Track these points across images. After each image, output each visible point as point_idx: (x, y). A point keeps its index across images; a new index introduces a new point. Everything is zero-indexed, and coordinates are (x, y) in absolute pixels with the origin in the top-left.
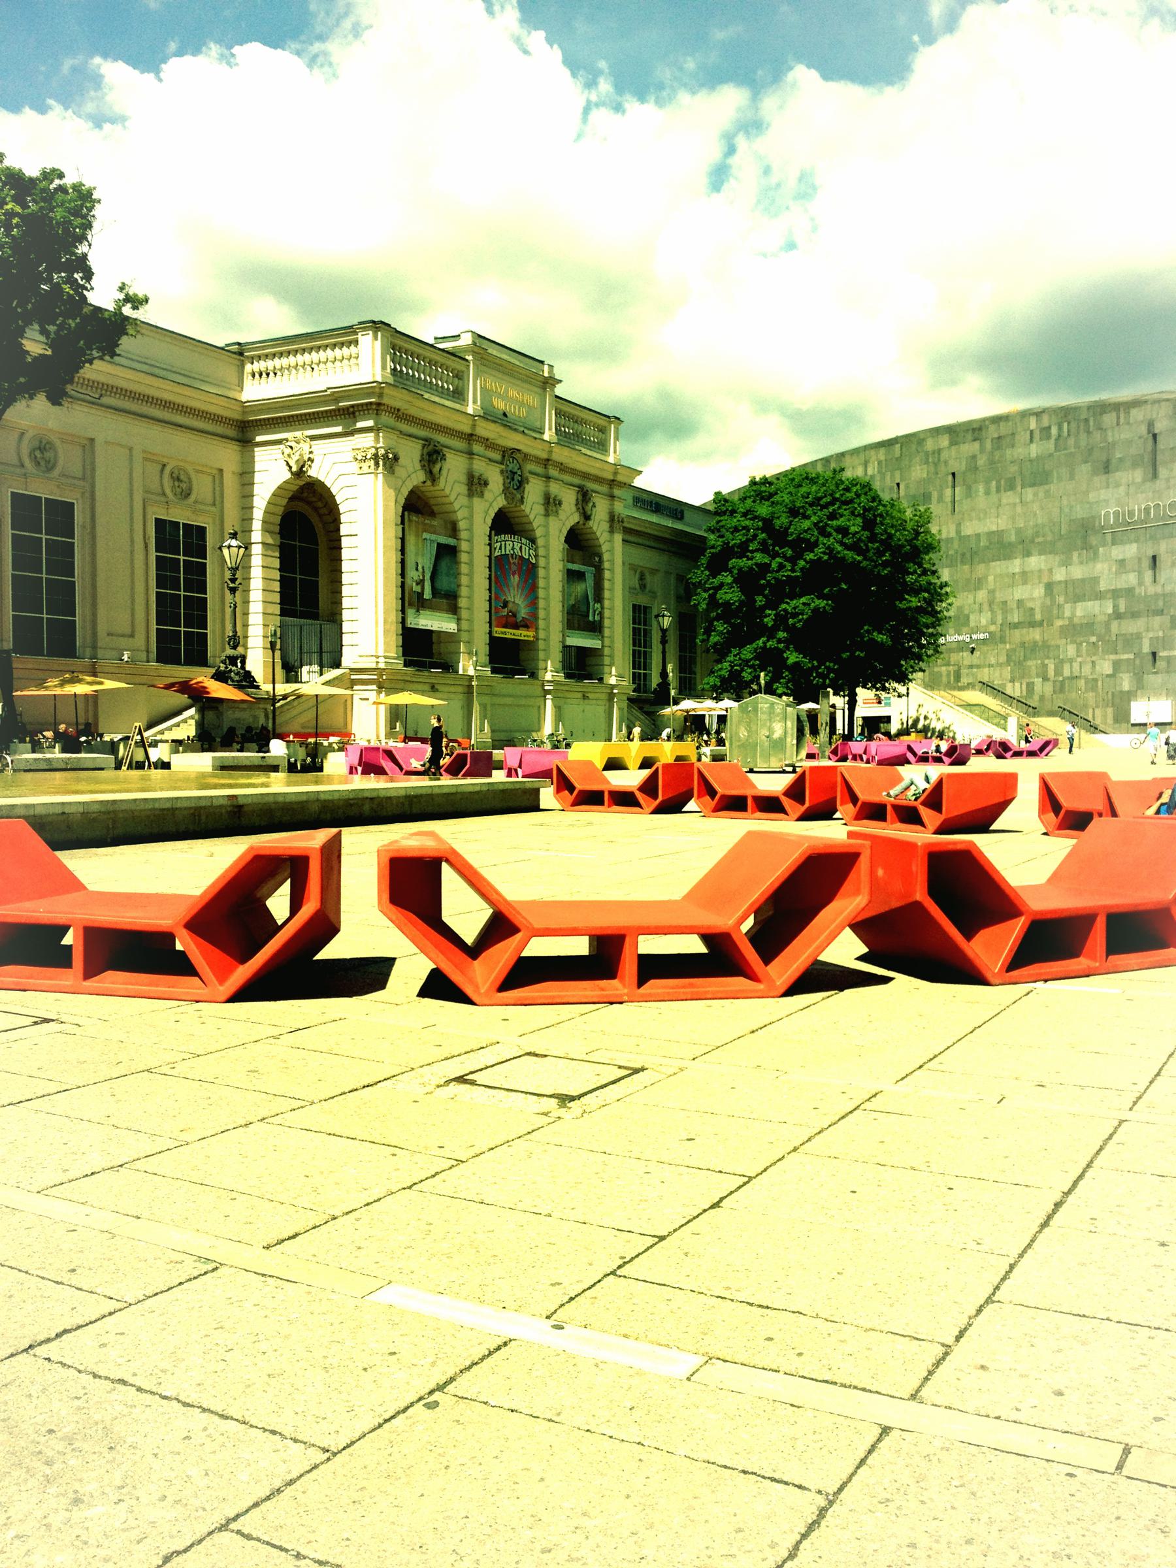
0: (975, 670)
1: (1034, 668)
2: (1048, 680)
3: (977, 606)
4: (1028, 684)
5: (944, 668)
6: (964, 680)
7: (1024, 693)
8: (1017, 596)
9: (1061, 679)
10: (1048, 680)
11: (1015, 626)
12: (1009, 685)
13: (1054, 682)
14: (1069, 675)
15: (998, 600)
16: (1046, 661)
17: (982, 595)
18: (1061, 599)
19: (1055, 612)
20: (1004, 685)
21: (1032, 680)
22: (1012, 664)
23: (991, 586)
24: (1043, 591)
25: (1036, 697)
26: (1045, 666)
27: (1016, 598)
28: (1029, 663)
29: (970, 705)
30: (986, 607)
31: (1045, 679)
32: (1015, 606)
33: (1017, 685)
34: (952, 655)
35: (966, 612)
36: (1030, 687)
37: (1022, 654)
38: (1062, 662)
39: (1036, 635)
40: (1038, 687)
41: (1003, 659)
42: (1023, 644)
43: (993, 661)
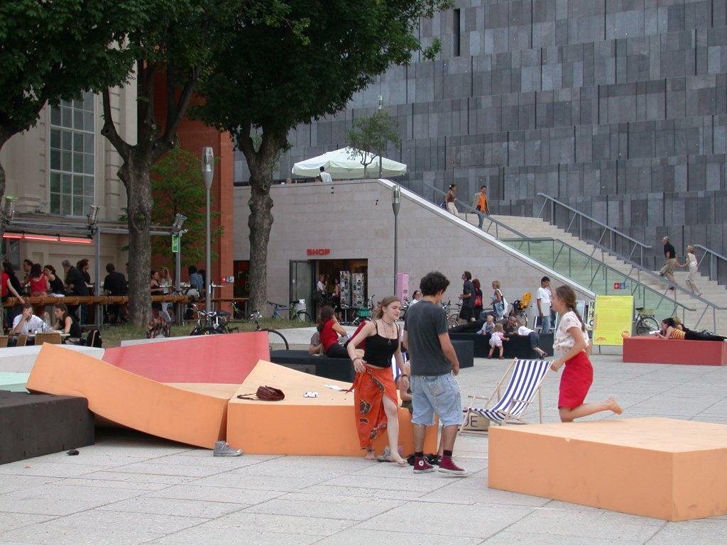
0: (531, 176)
1: (646, 172)
2: (674, 196)
3: (534, 54)
4: (633, 203)
5: (472, 172)
6: (511, 196)
7: (627, 221)
8: (614, 32)
9: (701, 194)
10: (674, 196)
11: (606, 92)
12: (598, 205)
13: (687, 201)
14: (717, 188)
15: (574, 42)
16: (673, 160)
17: (543, 30)
18: (703, 37)
19: (689, 60)
20: (588, 207)
21: (643, 197)
22: (604, 166)
23: (562, 14)
24: (665, 22)
25: (651, 231)
26: (669, 169)
27: (611, 37)
28: (636, 162)
29: (529, 240)
30: (552, 52)
31: (670, 195)
32: (608, 50)
33: (614, 205)
34: (488, 145)
35: (515, 64)
36: (640, 209)
37: (624, 145)
38: (704, 161)
39: (653, 110)
40: (654, 211)
41: (584, 155)
42: (626, 128)
43: (566, 160)
